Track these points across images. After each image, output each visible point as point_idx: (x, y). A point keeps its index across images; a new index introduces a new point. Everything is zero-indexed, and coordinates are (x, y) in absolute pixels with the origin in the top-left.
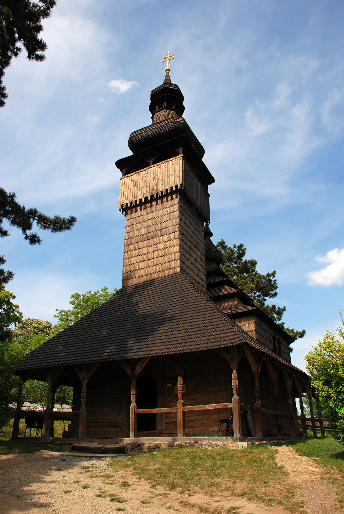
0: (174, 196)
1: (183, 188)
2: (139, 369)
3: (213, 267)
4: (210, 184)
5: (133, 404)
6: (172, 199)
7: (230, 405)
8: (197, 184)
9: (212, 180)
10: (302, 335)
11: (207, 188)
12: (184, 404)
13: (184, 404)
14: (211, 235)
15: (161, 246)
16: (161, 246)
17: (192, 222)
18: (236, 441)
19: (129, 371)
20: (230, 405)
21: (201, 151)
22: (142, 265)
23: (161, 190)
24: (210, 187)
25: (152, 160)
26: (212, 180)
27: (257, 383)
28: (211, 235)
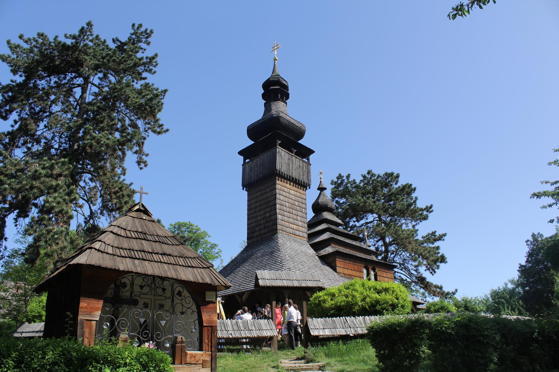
8: (297, 161)
9: (312, 152)
11: (308, 159)
16: (268, 214)
17: (292, 192)
19: (240, 301)
22: (257, 228)
24: (311, 157)
26: (312, 152)
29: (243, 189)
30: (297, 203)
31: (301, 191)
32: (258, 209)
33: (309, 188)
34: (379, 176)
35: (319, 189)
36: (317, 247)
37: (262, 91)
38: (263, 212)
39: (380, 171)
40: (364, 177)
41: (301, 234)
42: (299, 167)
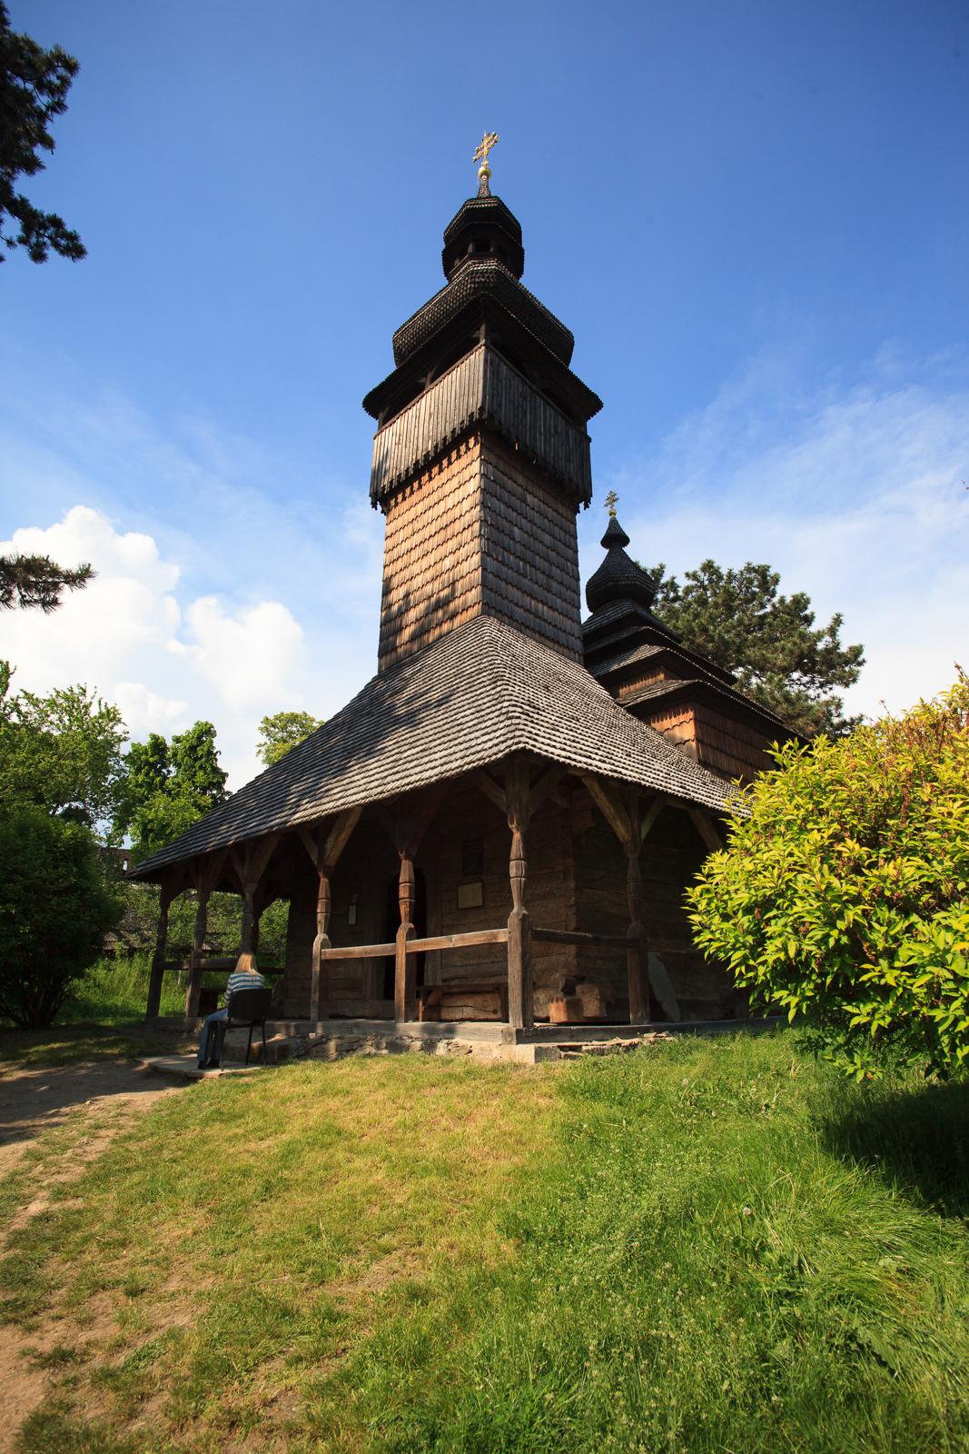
0: (472, 441)
1: (485, 416)
2: (335, 846)
3: (626, 608)
4: (593, 414)
5: (320, 937)
6: (468, 449)
7: (502, 936)
9: (594, 404)
10: (79, 578)
12: (410, 936)
13: (410, 936)
14: (626, 541)
15: (448, 563)
17: (529, 498)
18: (510, 1042)
19: (314, 857)
20: (502, 936)
21: (563, 342)
23: (443, 436)
25: (430, 375)
26: (594, 404)
27: (632, 869)
28: (626, 541)
29: (374, 505)
30: (547, 539)
31: (562, 509)
32: (415, 555)
33: (586, 506)
34: (731, 576)
35: (605, 543)
36: (611, 683)
37: (443, 246)
38: (432, 558)
39: (731, 563)
40: (694, 576)
41: (562, 637)
42: (556, 432)
